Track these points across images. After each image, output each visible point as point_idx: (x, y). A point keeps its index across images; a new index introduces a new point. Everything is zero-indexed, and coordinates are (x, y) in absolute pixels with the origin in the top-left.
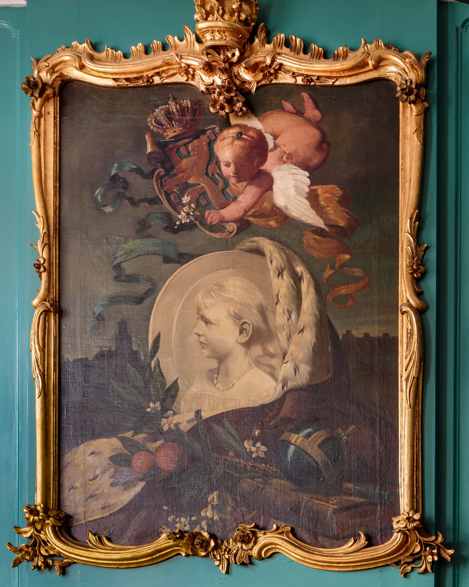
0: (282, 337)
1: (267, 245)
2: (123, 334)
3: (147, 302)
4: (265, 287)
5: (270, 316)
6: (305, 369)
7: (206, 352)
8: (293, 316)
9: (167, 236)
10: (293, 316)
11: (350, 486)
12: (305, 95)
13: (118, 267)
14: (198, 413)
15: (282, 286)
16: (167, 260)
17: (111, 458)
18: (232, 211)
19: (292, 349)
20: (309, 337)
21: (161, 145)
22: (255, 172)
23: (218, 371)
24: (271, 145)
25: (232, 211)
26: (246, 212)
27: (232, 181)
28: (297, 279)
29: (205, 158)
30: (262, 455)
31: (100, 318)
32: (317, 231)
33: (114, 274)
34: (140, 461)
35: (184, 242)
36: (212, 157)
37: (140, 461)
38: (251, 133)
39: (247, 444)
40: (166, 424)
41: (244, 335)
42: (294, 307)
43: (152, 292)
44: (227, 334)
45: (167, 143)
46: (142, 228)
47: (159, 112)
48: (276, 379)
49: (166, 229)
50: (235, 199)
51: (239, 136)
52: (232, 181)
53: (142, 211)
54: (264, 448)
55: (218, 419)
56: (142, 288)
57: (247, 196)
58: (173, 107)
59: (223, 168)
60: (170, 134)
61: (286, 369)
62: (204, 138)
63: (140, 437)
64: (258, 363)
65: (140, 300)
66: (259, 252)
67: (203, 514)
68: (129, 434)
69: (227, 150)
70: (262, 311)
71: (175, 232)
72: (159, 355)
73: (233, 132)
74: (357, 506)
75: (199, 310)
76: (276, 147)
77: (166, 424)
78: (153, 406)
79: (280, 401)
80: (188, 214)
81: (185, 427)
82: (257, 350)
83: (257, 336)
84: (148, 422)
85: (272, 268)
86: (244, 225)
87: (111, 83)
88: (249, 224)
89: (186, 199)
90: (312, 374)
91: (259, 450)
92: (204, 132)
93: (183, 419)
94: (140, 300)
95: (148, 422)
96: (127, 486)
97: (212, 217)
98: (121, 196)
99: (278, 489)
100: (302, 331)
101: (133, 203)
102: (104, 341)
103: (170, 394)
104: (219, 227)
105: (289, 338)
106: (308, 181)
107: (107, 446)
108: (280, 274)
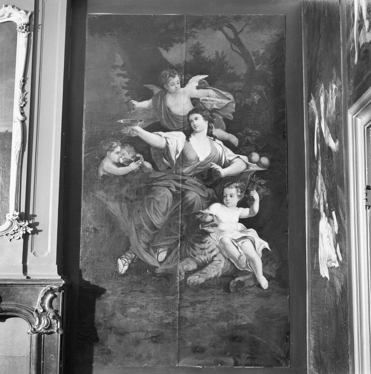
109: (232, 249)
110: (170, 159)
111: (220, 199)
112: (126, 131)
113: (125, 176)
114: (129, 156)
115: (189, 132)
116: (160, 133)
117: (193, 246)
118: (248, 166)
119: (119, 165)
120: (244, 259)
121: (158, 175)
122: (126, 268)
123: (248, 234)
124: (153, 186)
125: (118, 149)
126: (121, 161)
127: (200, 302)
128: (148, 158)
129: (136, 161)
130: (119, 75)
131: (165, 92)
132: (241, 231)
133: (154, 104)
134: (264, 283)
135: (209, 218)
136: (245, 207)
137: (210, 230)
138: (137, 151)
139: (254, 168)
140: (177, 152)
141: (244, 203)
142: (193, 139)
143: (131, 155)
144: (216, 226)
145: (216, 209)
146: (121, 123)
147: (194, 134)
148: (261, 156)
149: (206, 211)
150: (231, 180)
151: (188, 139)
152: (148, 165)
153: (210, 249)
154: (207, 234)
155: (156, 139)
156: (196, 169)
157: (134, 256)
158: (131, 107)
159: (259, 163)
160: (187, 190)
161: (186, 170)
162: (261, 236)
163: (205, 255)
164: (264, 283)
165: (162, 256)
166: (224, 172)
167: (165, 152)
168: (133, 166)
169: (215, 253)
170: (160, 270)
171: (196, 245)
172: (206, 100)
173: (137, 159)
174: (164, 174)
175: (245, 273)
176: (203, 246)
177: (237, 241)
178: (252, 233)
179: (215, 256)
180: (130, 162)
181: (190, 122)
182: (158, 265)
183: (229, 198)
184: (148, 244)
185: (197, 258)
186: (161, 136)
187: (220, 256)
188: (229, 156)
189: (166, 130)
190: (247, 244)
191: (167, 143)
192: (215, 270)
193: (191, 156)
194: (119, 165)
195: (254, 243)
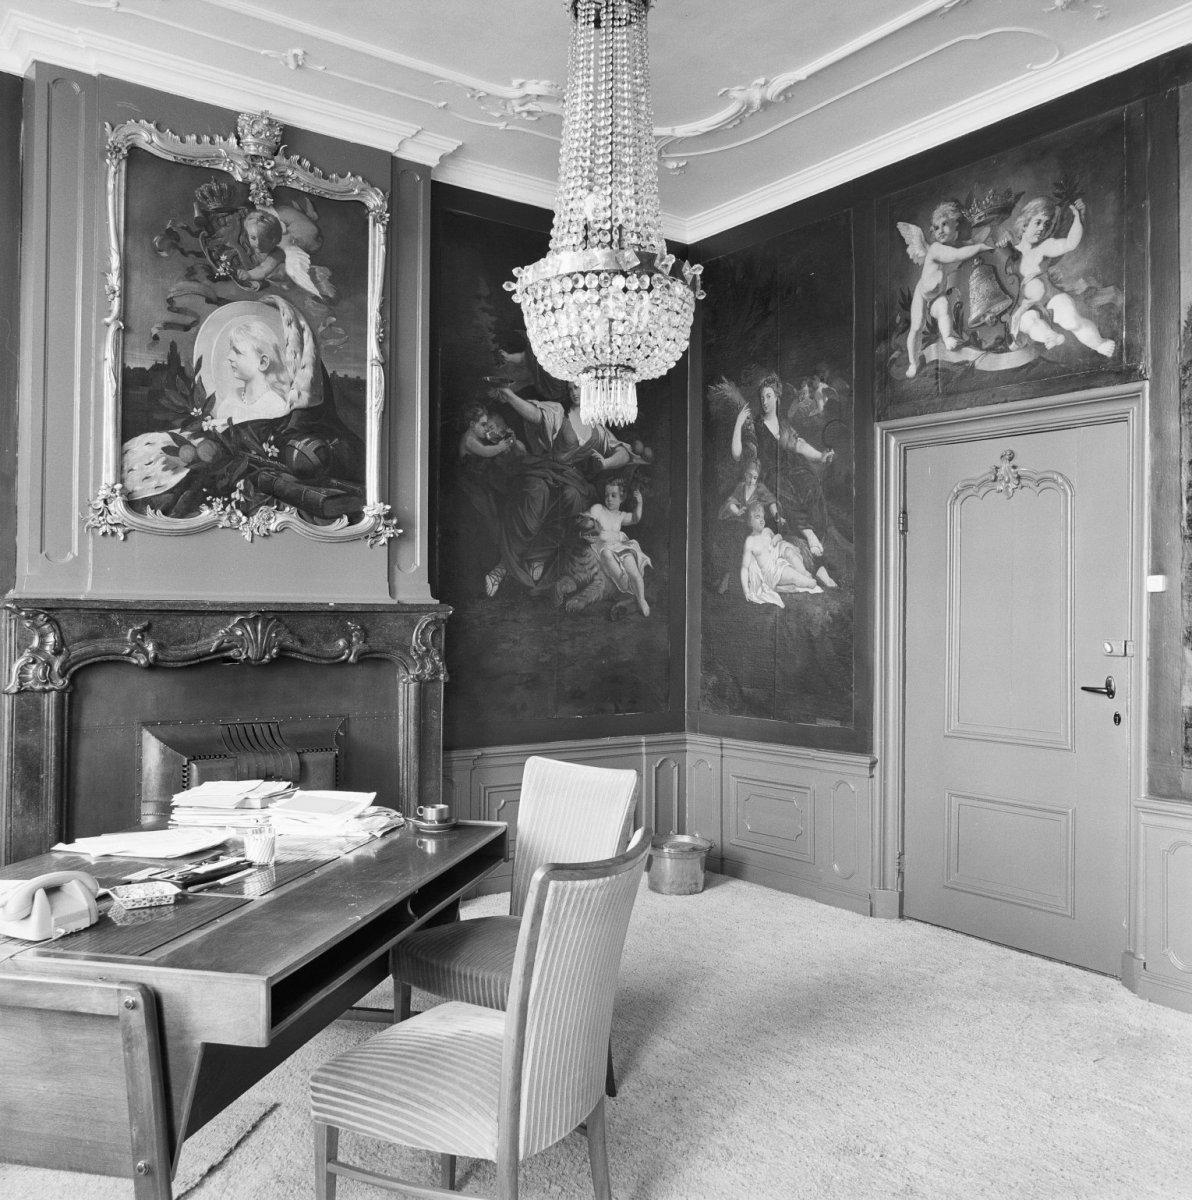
0: (290, 370)
4: (279, 333)
5: (282, 354)
6: (306, 396)
8: (298, 355)
10: (298, 355)
11: (334, 481)
14: (230, 420)
15: (291, 333)
16: (209, 301)
17: (164, 449)
18: (257, 273)
19: (296, 380)
20: (308, 372)
21: (205, 212)
24: (284, 230)
25: (257, 273)
27: (257, 250)
28: (301, 330)
30: (275, 455)
31: (156, 338)
32: (315, 298)
34: (186, 453)
35: (222, 289)
36: (243, 231)
37: (186, 453)
39: (265, 446)
40: (206, 426)
43: (197, 323)
44: (251, 364)
46: (190, 274)
48: (284, 399)
50: (259, 264)
51: (262, 219)
52: (257, 250)
53: (191, 260)
54: (277, 450)
56: (189, 320)
57: (267, 265)
58: (215, 188)
59: (251, 240)
60: (212, 206)
61: (292, 394)
63: (186, 434)
64: (273, 386)
65: (187, 328)
66: (275, 306)
67: (233, 496)
68: (177, 431)
69: (253, 228)
70: (277, 350)
71: (215, 281)
73: (258, 215)
74: (338, 496)
75: (231, 341)
76: (287, 232)
77: (206, 426)
78: (196, 411)
79: (288, 417)
81: (220, 430)
82: (272, 377)
83: (273, 368)
84: (189, 422)
86: (265, 285)
87: (171, 158)
89: (223, 258)
90: (311, 400)
91: (273, 451)
92: (237, 210)
93: (217, 423)
94: (187, 328)
95: (189, 422)
96: (175, 469)
97: (242, 274)
98: (175, 246)
101: (183, 252)
102: (160, 356)
103: (209, 403)
104: (246, 283)
105: (295, 372)
107: (162, 438)
108: (289, 324)
109: (614, 564)
110: (545, 439)
111: (602, 499)
112: (492, 393)
113: (493, 458)
114: (497, 431)
116: (536, 402)
117: (572, 560)
118: (631, 457)
119: (486, 442)
120: (626, 576)
121: (533, 460)
122: (496, 587)
123: (631, 547)
124: (527, 475)
125: (484, 419)
127: (580, 634)
128: (520, 436)
129: (506, 438)
130: (484, 310)
132: (623, 543)
134: (646, 609)
135: (590, 524)
136: (627, 511)
137: (591, 539)
138: (508, 424)
139: (638, 460)
140: (554, 430)
141: (627, 506)
143: (500, 430)
144: (597, 534)
145: (597, 511)
146: (486, 382)
148: (645, 446)
149: (587, 514)
150: (615, 473)
152: (521, 445)
153: (591, 565)
154: (588, 544)
155: (528, 408)
156: (575, 456)
157: (504, 571)
158: (500, 361)
159: (642, 455)
160: (566, 484)
161: (564, 457)
162: (643, 550)
163: (585, 572)
164: (646, 609)
165: (537, 573)
166: (606, 462)
167: (540, 427)
168: (502, 445)
169: (596, 570)
170: (536, 591)
171: (576, 558)
173: (507, 436)
174: (539, 459)
175: (627, 596)
176: (583, 560)
177: (619, 555)
178: (635, 545)
179: (596, 574)
180: (499, 439)
182: (532, 584)
183: (611, 497)
184: (521, 556)
185: (576, 577)
186: (536, 405)
187: (601, 574)
188: (612, 442)
189: (542, 399)
190: (630, 559)
192: (596, 592)
193: (570, 438)
195: (636, 558)
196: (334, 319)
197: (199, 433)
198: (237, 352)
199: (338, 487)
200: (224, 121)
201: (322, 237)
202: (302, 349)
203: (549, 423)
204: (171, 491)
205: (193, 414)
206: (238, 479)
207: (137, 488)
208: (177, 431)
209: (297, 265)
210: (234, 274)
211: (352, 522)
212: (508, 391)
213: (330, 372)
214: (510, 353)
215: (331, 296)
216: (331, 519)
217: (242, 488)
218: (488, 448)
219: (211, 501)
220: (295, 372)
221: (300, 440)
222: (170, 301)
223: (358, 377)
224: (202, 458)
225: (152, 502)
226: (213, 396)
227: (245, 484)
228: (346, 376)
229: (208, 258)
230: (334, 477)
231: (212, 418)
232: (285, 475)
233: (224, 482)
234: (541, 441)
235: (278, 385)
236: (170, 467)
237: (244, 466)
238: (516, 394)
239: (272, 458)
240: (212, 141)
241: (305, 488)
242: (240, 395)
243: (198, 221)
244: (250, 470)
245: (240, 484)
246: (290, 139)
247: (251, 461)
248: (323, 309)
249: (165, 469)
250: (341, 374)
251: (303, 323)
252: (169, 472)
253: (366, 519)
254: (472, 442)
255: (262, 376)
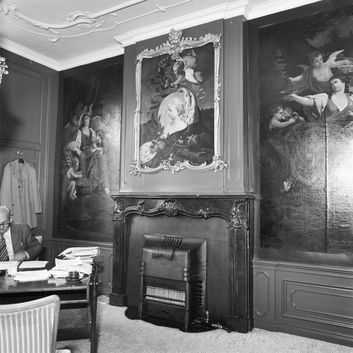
0: (187, 112)
1: (184, 89)
2: (153, 117)
3: (158, 108)
4: (183, 100)
5: (184, 107)
6: (192, 120)
7: (170, 118)
8: (190, 106)
9: (162, 91)
10: (190, 106)
11: (202, 149)
12: (193, 50)
13: (152, 100)
14: (168, 133)
15: (187, 99)
17: (150, 147)
18: (176, 82)
19: (189, 115)
20: (193, 111)
21: (162, 69)
22: (181, 72)
23: (172, 123)
25: (176, 82)
26: (179, 82)
27: (176, 75)
28: (190, 97)
29: (171, 70)
30: (182, 143)
31: (148, 113)
32: (196, 84)
33: (151, 102)
34: (156, 147)
35: (166, 92)
36: (172, 70)
38: (181, 62)
39: (179, 140)
40: (161, 137)
41: (179, 113)
42: (190, 104)
43: (159, 105)
44: (175, 113)
45: (163, 69)
46: (157, 90)
47: (161, 62)
48: (185, 122)
49: (162, 89)
50: (177, 79)
51: (178, 64)
52: (176, 75)
53: (158, 85)
54: (183, 141)
55: (172, 135)
56: (157, 104)
57: (180, 78)
59: (175, 72)
60: (164, 66)
62: (170, 66)
63: (156, 141)
64: (181, 119)
65: (156, 107)
66: (182, 91)
67: (169, 159)
68: (153, 141)
69: (175, 68)
70: (183, 106)
72: (160, 120)
73: (177, 63)
74: (204, 154)
75: (169, 108)
76: (186, 64)
77: (161, 137)
79: (186, 129)
80: (167, 85)
81: (165, 137)
82: (181, 116)
83: (181, 113)
85: (185, 95)
86: (179, 85)
87: (151, 57)
88: (180, 84)
89: (166, 81)
90: (194, 121)
91: (181, 141)
93: (165, 136)
94: (156, 107)
97: (172, 85)
98: (153, 83)
99: (186, 152)
100: (191, 110)
101: (156, 84)
102: (149, 118)
105: (189, 112)
106: (193, 72)
107: (149, 144)
108: (187, 96)
110: (317, 113)
112: (285, 98)
114: (288, 115)
115: (331, 91)
116: (310, 96)
119: (282, 121)
122: (289, 187)
125: (281, 111)
126: (283, 118)
128: (302, 114)
129: (293, 117)
130: (279, 63)
131: (312, 67)
133: (304, 77)
138: (294, 110)
140: (322, 107)
142: (334, 97)
143: (290, 114)
146: (282, 94)
147: (334, 94)
151: (330, 98)
152: (302, 118)
155: (306, 100)
158: (288, 82)
167: (313, 108)
168: (292, 120)
172: (343, 68)
180: (289, 118)
181: (331, 85)
186: (310, 98)
189: (313, 94)
191: (315, 102)
193: (332, 108)
194: (282, 121)
196: (202, 89)
197: (160, 140)
198: (171, 111)
199: (204, 151)
200: (164, 38)
201: (198, 61)
202: (191, 103)
203: (319, 104)
204: (152, 160)
205: (158, 134)
206: (171, 153)
207: (143, 160)
208: (153, 141)
209: (189, 75)
210: (170, 85)
211: (208, 164)
212: (294, 95)
213: (200, 109)
214: (293, 77)
215: (201, 81)
216: (200, 164)
217: (172, 156)
218: (284, 123)
219: (163, 162)
220: (189, 112)
221: (190, 136)
222: (152, 100)
223: (211, 108)
224: (160, 148)
225: (147, 164)
226: (164, 127)
227: (173, 154)
228: (207, 109)
229: (162, 83)
230: (202, 148)
231: (163, 134)
232: (185, 149)
233: (166, 155)
234: (314, 114)
235: (183, 118)
236: (152, 152)
237: (173, 148)
238: (300, 95)
239: (181, 144)
240: (163, 46)
241: (192, 153)
242: (171, 125)
243: (160, 73)
244: (174, 149)
245: (171, 155)
246: (186, 33)
247: (176, 146)
248: (198, 87)
249: (150, 153)
250: (205, 109)
251: (191, 94)
252: (151, 154)
253: (214, 162)
254: (275, 122)
255: (178, 116)
